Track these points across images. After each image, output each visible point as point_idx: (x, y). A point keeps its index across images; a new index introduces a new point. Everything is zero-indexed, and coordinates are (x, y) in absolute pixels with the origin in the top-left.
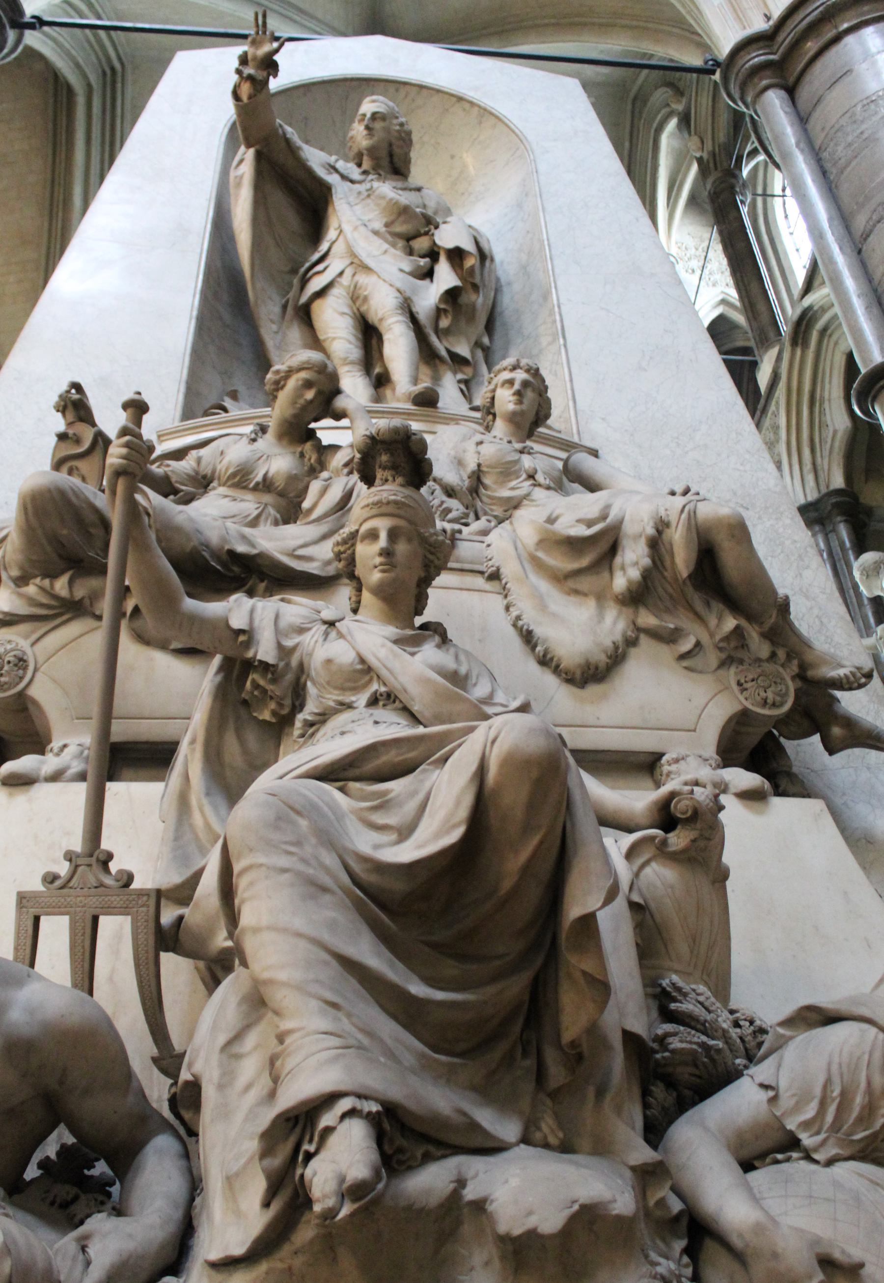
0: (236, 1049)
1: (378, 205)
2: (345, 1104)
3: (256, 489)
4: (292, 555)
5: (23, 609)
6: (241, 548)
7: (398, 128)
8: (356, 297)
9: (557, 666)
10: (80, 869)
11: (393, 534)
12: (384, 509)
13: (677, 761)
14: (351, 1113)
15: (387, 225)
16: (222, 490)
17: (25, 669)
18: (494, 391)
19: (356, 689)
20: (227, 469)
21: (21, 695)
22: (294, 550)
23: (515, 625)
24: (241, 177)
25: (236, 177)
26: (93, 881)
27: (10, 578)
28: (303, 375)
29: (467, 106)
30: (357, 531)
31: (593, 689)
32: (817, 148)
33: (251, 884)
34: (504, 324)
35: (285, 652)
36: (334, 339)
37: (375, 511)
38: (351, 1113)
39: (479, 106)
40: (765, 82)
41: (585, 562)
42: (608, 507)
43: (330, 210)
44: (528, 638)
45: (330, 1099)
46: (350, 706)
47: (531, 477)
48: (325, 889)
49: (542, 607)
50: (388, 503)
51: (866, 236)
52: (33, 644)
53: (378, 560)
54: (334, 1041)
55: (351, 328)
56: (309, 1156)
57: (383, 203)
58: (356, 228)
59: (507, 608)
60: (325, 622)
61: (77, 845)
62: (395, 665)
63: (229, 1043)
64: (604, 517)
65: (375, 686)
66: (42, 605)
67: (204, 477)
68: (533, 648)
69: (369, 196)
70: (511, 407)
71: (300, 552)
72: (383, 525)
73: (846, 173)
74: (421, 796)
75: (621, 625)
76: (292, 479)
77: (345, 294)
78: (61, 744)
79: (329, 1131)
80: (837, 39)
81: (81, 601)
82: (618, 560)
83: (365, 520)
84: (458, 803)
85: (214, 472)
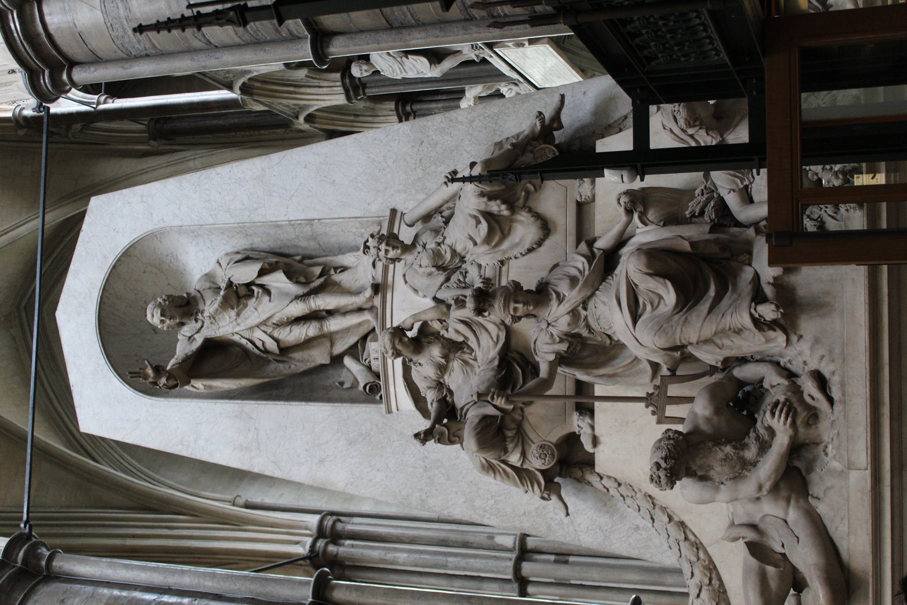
0: (721, 346)
1: (220, 313)
2: (753, 311)
3: (447, 361)
4: (497, 343)
5: (519, 449)
6: (496, 363)
7: (167, 303)
9: (542, 240)
10: (652, 402)
11: (516, 302)
12: (507, 305)
13: (581, 196)
14: (755, 309)
15: (233, 309)
16: (446, 377)
17: (545, 445)
18: (387, 258)
19: (579, 315)
20: (438, 374)
21: (555, 445)
22: (494, 342)
23: (524, 255)
24: (205, 386)
25: (205, 389)
26: (656, 398)
27: (504, 455)
28: (397, 342)
29: (119, 263)
30: (512, 315)
31: (551, 226)
32: (125, 56)
33: (685, 339)
34: (280, 248)
35: (561, 341)
36: (306, 335)
37: (507, 309)
38: (755, 309)
39: (121, 256)
40: (65, 77)
41: (497, 226)
42: (470, 215)
44: (530, 250)
45: (751, 315)
46: (586, 317)
47: (439, 244)
48: (686, 319)
49: (517, 245)
50: (504, 303)
51: (209, 42)
52: (534, 443)
53: (525, 308)
54: (734, 315)
55: (299, 326)
56: (765, 320)
57: (220, 310)
58: (238, 325)
59: (516, 258)
60: (548, 327)
61: (643, 405)
62: (573, 301)
63: (719, 348)
64: (475, 217)
65: (580, 308)
66: (518, 441)
67: (437, 385)
68: (533, 248)
69: (214, 318)
70: (399, 251)
71: (495, 339)
72: (512, 305)
74: (648, 292)
75: (524, 214)
76: (443, 347)
77: (277, 330)
78: (577, 427)
79: (760, 315)
80: (49, 36)
81: (516, 425)
82: (495, 213)
83: (509, 312)
84: (657, 281)
85: (435, 380)
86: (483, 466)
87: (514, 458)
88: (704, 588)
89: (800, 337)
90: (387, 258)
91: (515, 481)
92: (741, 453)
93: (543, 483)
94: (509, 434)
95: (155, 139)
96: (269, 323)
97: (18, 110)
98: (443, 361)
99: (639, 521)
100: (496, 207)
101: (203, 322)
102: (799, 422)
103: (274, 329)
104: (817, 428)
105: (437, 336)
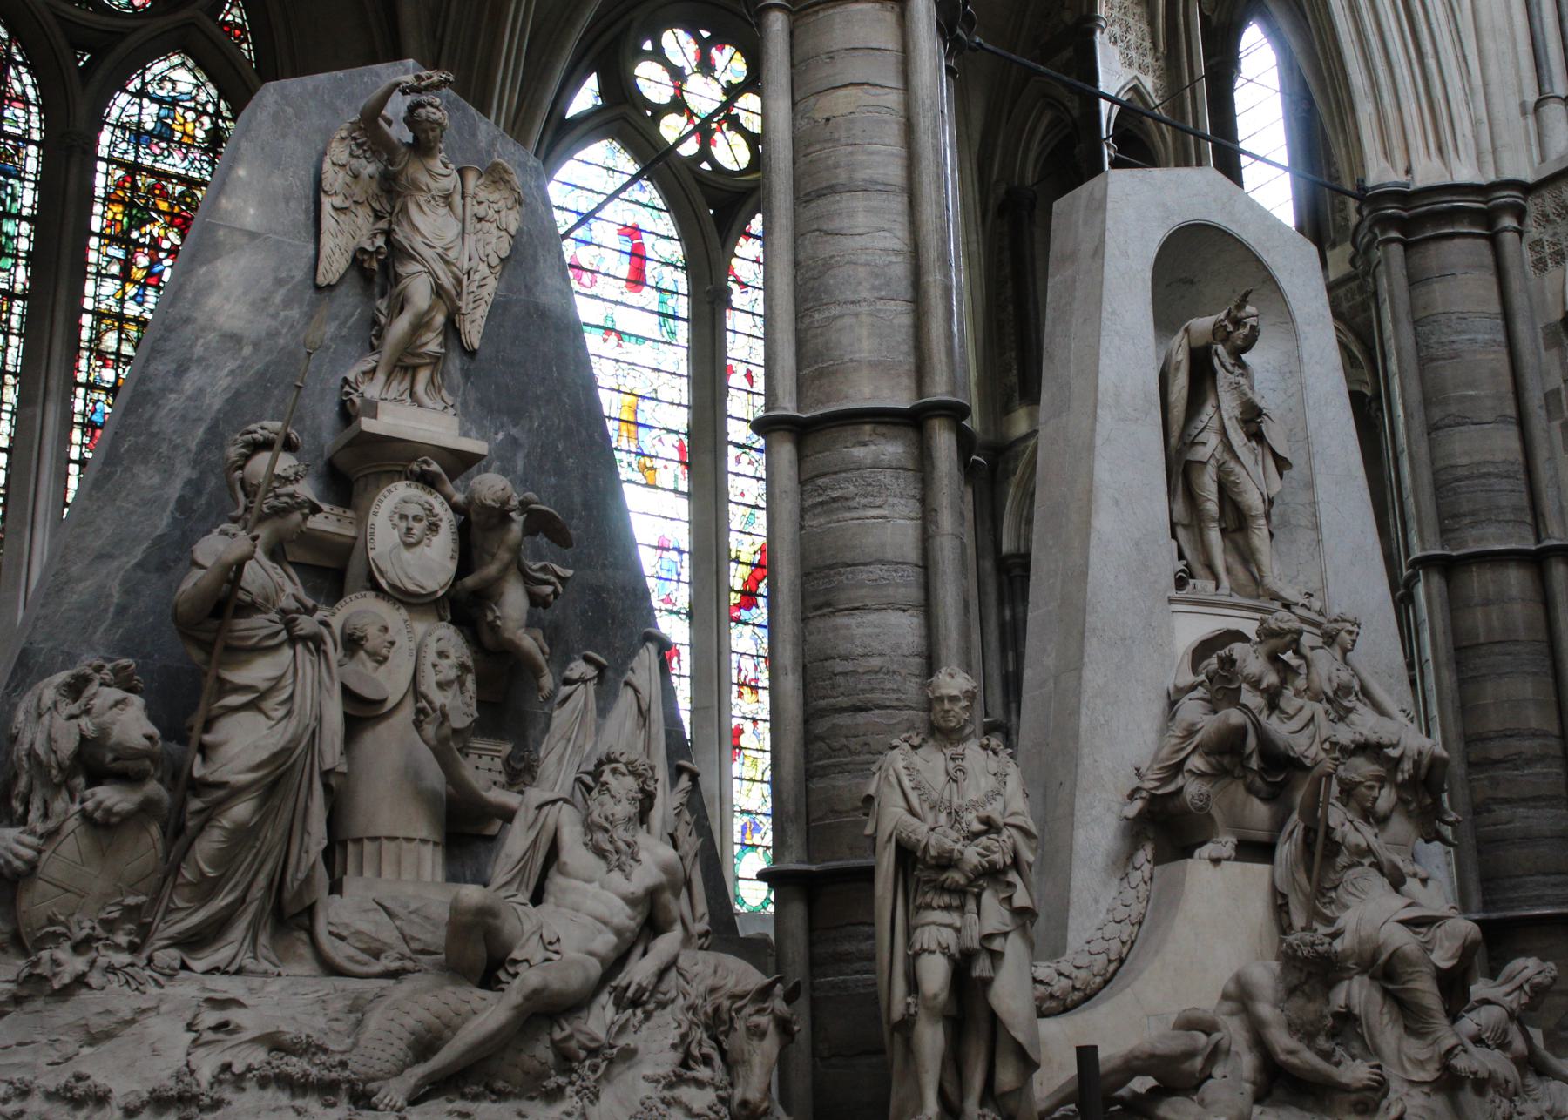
3: (1263, 691)
8: (1220, 467)
18: (1340, 630)
24: (1179, 363)
43: (1209, 384)
46: (1362, 865)
73: (1435, 364)
86: (1193, 725)
87: (1197, 763)
88: (1070, 982)
89: (1428, 1095)
90: (1340, 630)
91: (1168, 760)
92: (1323, 1033)
93: (1160, 792)
94: (1226, 761)
95: (1007, 192)
96: (1227, 457)
97: (1103, 24)
98: (1264, 685)
99: (1104, 907)
100: (1407, 766)
101: (1232, 373)
102: (1368, 1094)
103: (1218, 461)
104: (1350, 1113)
105: (1284, 682)
